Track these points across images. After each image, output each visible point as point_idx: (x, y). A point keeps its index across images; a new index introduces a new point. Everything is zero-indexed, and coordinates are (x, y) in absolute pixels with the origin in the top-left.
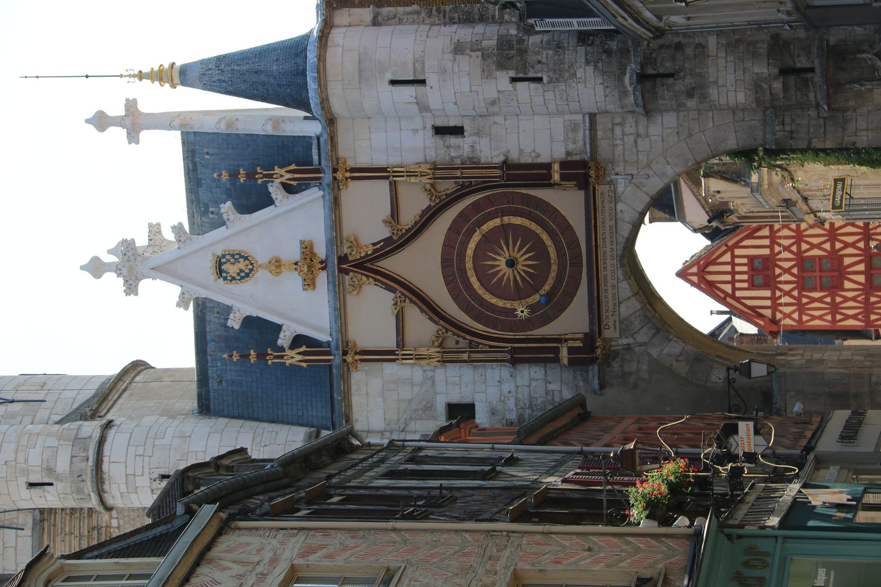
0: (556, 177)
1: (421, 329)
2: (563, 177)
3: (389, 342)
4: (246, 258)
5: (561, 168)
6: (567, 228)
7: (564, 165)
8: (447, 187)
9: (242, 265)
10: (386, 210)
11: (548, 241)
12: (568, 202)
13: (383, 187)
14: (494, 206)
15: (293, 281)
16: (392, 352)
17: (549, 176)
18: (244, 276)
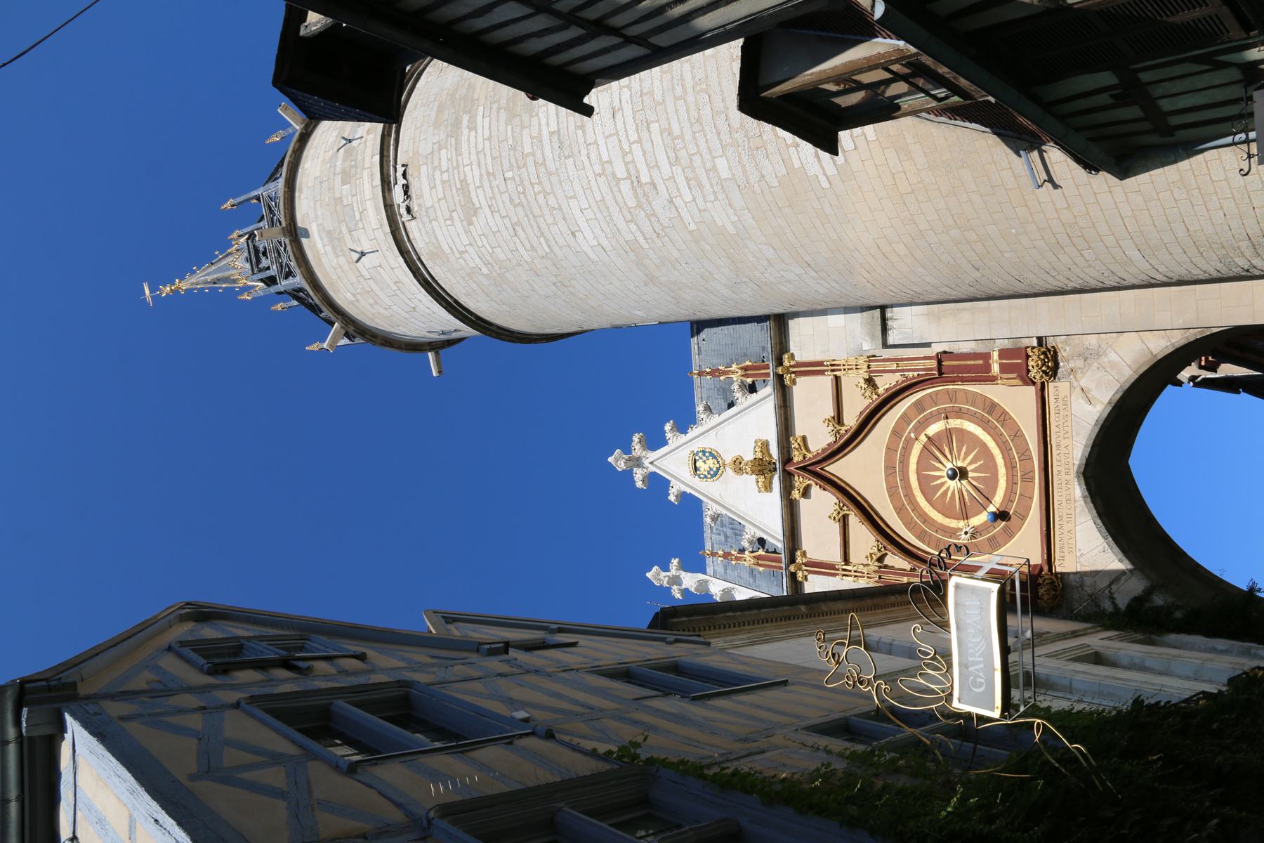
0: (996, 368)
1: (863, 539)
2: (1004, 368)
3: (835, 556)
4: (714, 457)
5: (1000, 357)
6: (1017, 434)
7: (1004, 353)
8: (886, 383)
9: (711, 463)
10: (830, 412)
11: (996, 452)
12: (1017, 401)
13: (826, 381)
14: (936, 405)
15: (750, 480)
16: (832, 566)
17: (987, 368)
18: (714, 474)
